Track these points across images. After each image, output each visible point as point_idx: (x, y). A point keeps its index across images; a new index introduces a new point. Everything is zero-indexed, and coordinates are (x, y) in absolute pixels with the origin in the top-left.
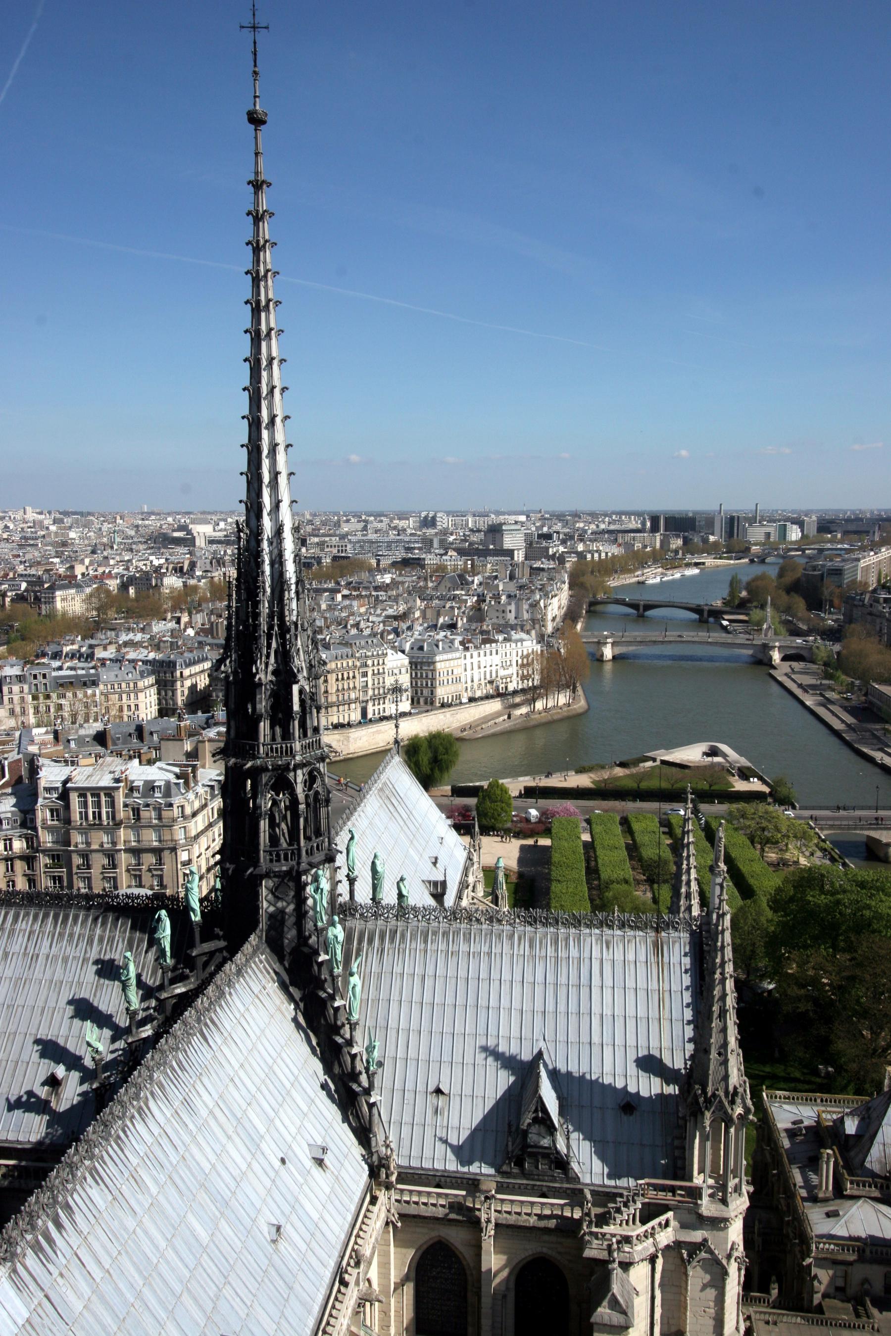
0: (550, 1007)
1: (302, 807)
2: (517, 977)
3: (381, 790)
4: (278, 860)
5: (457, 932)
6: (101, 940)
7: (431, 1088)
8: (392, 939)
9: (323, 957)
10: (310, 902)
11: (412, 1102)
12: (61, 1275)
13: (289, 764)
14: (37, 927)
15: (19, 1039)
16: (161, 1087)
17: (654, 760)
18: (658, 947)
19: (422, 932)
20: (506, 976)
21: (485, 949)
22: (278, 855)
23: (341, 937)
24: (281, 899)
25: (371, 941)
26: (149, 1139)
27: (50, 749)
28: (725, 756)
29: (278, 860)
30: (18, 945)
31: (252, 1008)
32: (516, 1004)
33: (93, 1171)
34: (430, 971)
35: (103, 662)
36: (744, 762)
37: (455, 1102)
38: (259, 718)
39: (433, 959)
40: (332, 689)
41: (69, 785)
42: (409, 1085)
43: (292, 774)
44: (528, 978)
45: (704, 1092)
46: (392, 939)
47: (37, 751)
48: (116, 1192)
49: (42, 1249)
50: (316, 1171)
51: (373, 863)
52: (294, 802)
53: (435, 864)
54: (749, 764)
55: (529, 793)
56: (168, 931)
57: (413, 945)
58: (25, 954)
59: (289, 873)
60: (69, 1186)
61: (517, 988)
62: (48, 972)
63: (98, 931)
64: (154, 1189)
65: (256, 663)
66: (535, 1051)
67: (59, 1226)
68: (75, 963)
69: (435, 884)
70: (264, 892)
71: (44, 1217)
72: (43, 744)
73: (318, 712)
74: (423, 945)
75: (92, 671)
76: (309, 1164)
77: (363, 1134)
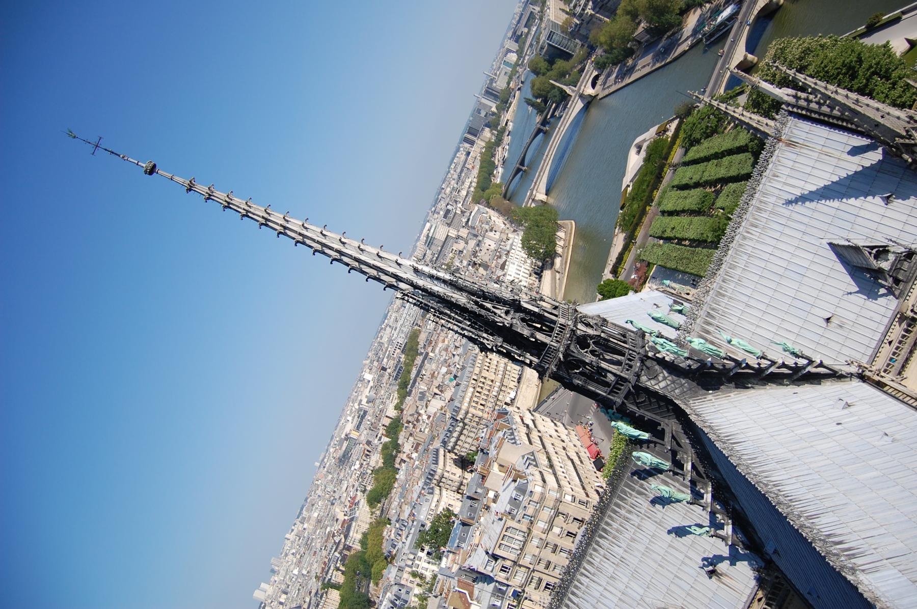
0: (802, 228)
1: (603, 335)
2: (773, 242)
4: (631, 366)
5: (727, 273)
6: (630, 512)
7: (824, 324)
8: (713, 317)
10: (667, 359)
11: (828, 341)
12: (875, 549)
13: (572, 330)
14: (602, 551)
15: (673, 587)
16: (763, 472)
17: (628, 186)
18: (791, 144)
20: (769, 249)
21: (745, 258)
23: (702, 341)
25: (708, 332)
26: (799, 485)
27: (459, 558)
28: (644, 141)
29: (631, 366)
30: (609, 568)
31: (725, 415)
32: (791, 250)
33: (808, 518)
35: (412, 514)
36: (653, 131)
37: (840, 312)
39: (738, 294)
40: (492, 377)
41: (490, 552)
42: (816, 338)
43: (579, 332)
44: (777, 235)
45: (902, 137)
46: (713, 317)
47: (458, 567)
48: (829, 510)
49: (853, 555)
50: (852, 409)
52: (598, 341)
54: (657, 127)
55: (614, 271)
56: (649, 456)
57: (723, 305)
58: (617, 565)
59: (642, 361)
60: (815, 531)
61: (781, 246)
62: (636, 553)
63: (623, 512)
64: (834, 491)
66: (828, 247)
67: (840, 543)
68: (638, 534)
70: (648, 383)
71: (832, 549)
72: (454, 561)
75: (415, 523)
76: (846, 411)
77: (835, 375)
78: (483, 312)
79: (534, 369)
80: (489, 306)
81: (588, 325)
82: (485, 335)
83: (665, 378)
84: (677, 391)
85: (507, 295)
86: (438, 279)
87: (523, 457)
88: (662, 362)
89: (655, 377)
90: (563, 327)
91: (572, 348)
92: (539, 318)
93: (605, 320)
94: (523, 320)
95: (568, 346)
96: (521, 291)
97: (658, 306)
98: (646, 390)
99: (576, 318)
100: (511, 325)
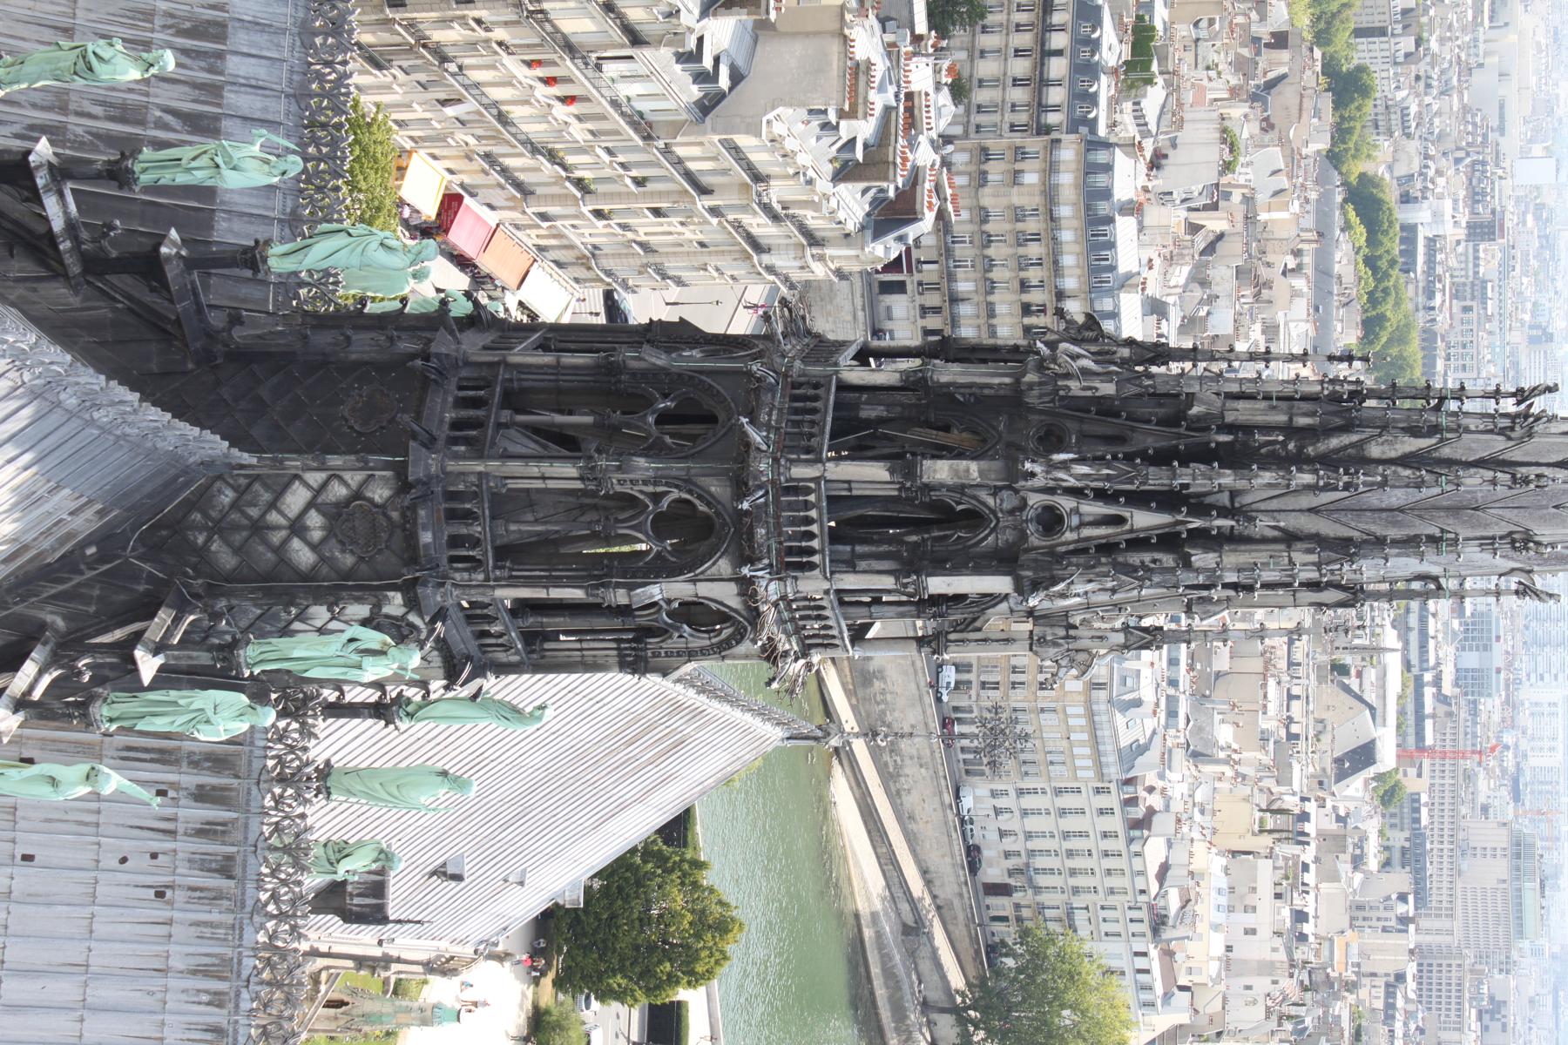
3: (677, 707)
4: (452, 515)
8: (203, 864)
9: (148, 665)
10: (320, 613)
13: (751, 560)
19: (225, 962)
22: (468, 516)
24: (330, 531)
25: (202, 795)
34: (103, 992)
38: (902, 460)
43: (724, 566)
51: (444, 774)
53: (441, 872)
56: (231, 181)
59: (412, 554)
65: (1082, 460)
69: (377, 888)
70: (354, 478)
73: (921, 641)
74: (177, 963)
78: (1157, 479)
79: (841, 345)
80: (1144, 520)
81: (694, 614)
82: (1108, 389)
83: (297, 527)
84: (227, 497)
85: (1077, 592)
86: (1410, 544)
87: (737, 77)
88: (331, 587)
89: (337, 514)
90: (794, 562)
91: (718, 488)
92: (914, 564)
93: (636, 664)
94: (975, 518)
95: (741, 488)
96: (1035, 643)
97: (441, 872)
98: (360, 445)
99: (755, 616)
100: (1014, 475)
